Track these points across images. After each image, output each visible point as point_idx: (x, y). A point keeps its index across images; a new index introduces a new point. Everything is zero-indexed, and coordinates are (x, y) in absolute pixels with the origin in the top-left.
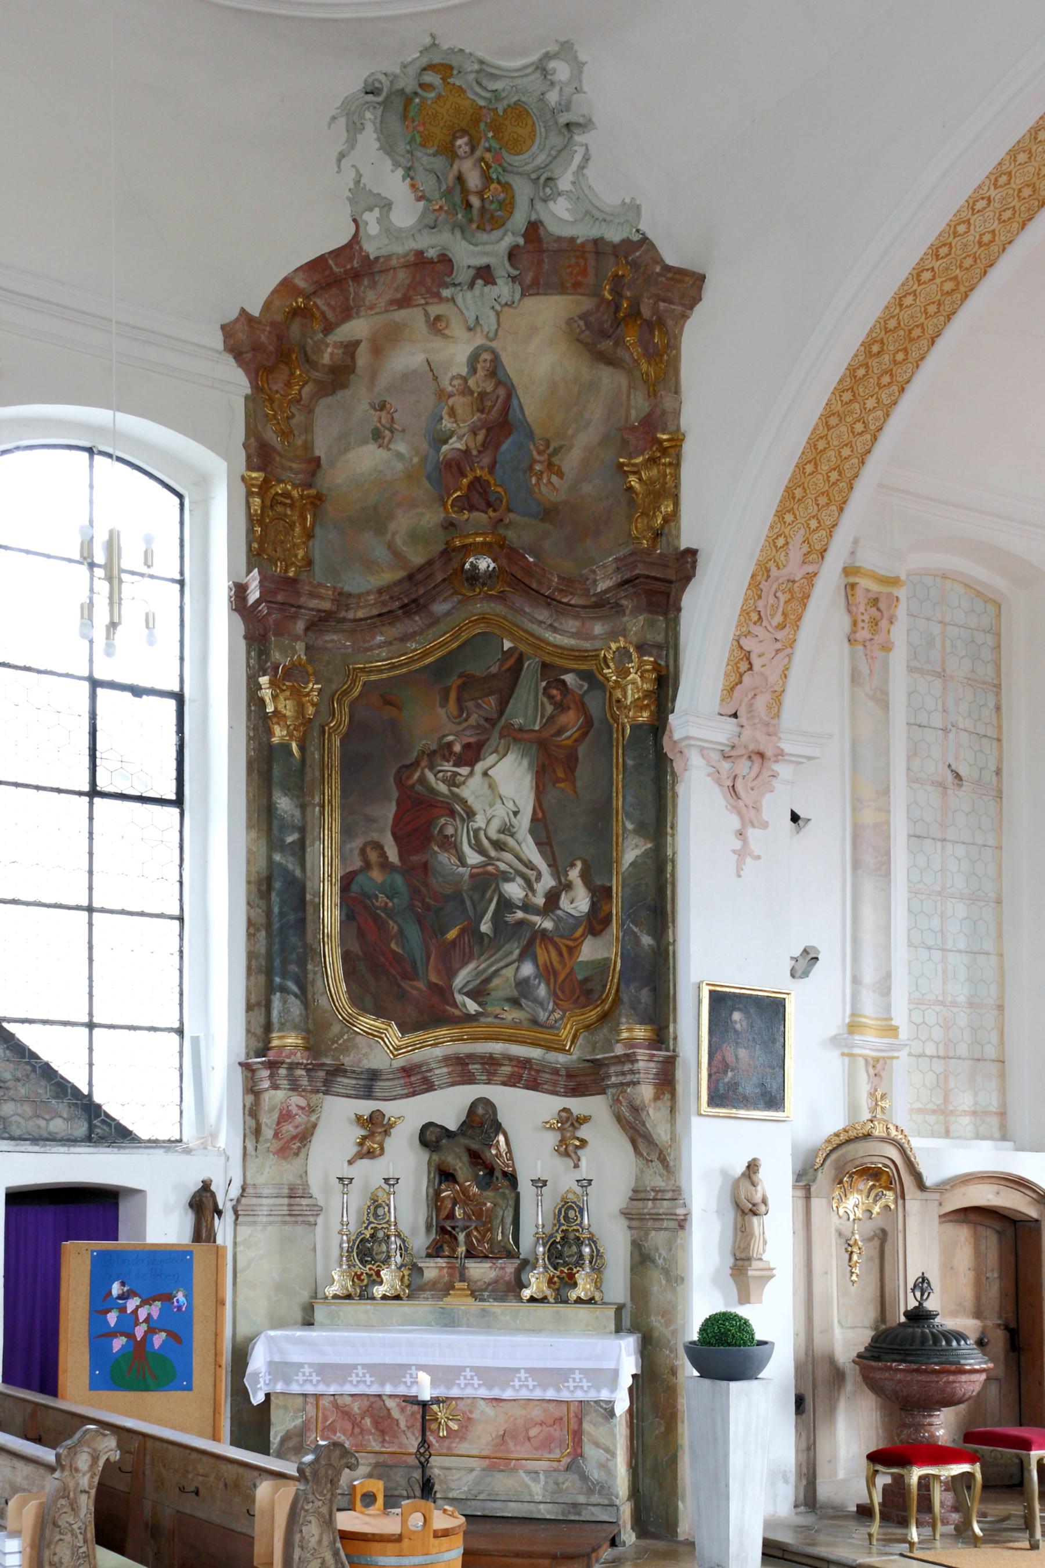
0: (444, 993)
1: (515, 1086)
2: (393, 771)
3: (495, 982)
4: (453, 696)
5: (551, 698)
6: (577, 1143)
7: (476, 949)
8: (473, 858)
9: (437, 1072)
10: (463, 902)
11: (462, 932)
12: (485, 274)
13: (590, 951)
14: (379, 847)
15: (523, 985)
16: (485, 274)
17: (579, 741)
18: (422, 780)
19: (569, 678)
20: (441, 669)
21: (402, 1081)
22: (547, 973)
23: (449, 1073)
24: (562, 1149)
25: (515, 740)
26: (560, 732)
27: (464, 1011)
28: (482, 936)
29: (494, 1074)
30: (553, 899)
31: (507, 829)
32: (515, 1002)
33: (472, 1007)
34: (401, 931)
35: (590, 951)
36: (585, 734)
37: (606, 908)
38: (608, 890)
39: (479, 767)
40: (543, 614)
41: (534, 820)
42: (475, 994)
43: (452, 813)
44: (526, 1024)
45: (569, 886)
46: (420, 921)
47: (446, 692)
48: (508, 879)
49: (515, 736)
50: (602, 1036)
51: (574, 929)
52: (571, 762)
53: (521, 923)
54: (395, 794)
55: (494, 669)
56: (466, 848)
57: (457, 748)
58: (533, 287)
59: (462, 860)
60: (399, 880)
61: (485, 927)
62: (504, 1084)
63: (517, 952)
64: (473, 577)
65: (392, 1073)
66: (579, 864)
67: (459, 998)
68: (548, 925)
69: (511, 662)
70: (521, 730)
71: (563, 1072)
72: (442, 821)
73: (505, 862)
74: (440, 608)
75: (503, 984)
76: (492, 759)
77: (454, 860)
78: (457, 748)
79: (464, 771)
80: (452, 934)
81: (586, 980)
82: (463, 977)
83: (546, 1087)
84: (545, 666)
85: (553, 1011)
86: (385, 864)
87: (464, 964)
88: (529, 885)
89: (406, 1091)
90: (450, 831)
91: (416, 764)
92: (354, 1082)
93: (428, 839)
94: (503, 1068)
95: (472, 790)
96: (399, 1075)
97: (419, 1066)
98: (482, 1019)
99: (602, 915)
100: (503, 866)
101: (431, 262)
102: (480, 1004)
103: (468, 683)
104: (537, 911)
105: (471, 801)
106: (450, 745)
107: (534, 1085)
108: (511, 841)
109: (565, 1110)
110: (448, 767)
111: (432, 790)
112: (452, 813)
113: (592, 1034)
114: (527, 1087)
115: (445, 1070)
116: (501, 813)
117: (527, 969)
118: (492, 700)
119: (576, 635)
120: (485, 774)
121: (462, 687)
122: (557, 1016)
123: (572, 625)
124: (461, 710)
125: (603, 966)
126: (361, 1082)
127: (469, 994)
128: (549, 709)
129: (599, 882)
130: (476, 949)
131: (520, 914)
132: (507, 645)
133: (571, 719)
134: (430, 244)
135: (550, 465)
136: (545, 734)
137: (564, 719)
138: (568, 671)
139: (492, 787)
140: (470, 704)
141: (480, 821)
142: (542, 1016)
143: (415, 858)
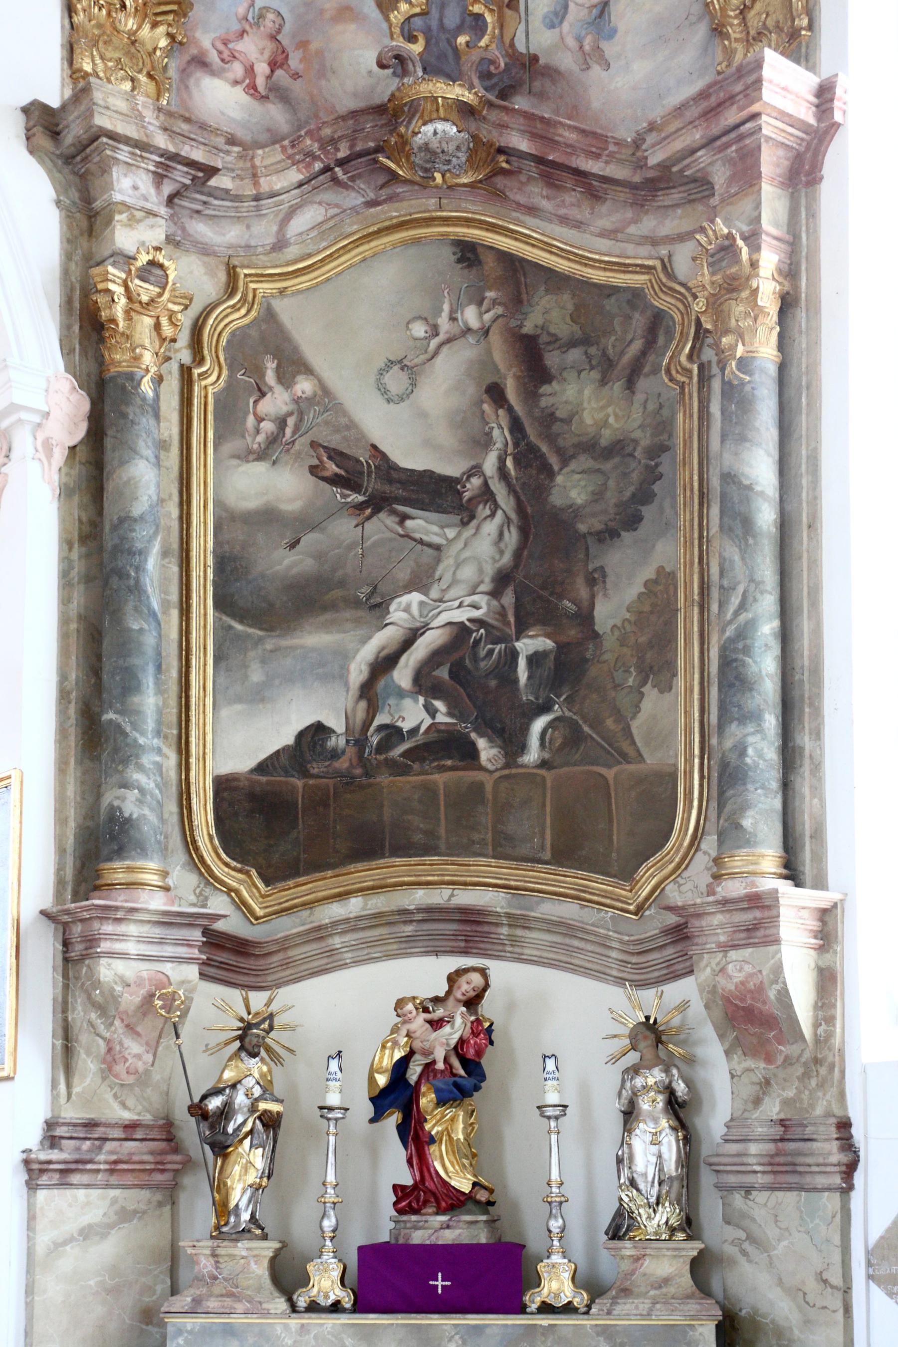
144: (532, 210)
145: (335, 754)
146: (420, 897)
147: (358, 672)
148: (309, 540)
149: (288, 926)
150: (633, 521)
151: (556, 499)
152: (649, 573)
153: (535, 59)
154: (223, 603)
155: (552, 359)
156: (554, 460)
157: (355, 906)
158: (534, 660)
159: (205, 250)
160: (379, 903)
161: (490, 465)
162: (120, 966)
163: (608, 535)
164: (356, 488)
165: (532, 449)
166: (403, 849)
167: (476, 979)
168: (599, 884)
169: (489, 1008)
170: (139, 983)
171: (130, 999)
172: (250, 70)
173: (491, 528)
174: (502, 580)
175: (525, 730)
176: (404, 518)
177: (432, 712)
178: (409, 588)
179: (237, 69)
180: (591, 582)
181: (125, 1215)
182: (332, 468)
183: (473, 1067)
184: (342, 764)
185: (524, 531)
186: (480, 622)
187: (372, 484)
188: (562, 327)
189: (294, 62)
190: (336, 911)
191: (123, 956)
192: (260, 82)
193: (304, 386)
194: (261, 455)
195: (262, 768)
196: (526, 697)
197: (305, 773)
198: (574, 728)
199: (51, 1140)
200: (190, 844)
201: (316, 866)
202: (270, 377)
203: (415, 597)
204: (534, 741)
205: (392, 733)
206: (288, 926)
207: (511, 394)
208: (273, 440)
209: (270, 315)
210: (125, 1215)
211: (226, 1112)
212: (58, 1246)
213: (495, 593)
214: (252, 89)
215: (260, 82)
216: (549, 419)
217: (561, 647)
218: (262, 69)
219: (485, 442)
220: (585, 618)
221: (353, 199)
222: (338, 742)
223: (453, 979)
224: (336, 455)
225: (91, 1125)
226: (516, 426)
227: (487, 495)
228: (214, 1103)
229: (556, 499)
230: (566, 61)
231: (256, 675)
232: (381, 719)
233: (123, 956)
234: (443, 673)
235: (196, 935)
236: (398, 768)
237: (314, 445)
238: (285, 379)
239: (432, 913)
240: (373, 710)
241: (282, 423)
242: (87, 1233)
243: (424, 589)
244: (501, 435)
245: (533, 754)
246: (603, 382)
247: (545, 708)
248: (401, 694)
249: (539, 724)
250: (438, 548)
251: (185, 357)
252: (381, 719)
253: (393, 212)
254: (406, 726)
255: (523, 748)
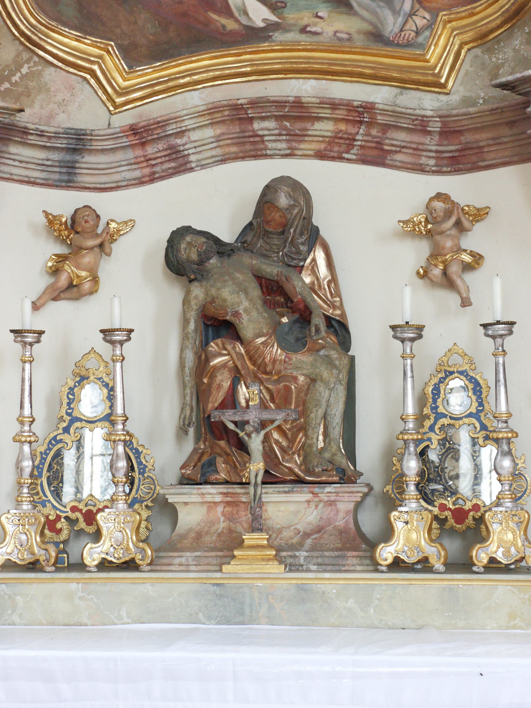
1: (340, 158)
6: (467, 258)
9: (195, 136)
21: (130, 155)
23: (218, 139)
24: (437, 272)
27: (244, 20)
44: (359, 40)
50: (510, 53)
62: (321, 156)
65: (113, 137)
71: (435, 126)
83: (399, 157)
85: (412, 14)
89: (137, 174)
92: (41, 155)
94: (318, 125)
96: (125, 141)
97: (162, 124)
98: (278, 36)
102: (273, 8)
109: (439, 196)
113: (490, 51)
114: (364, 161)
115: (209, 133)
122: (420, 22)
126: (56, 156)
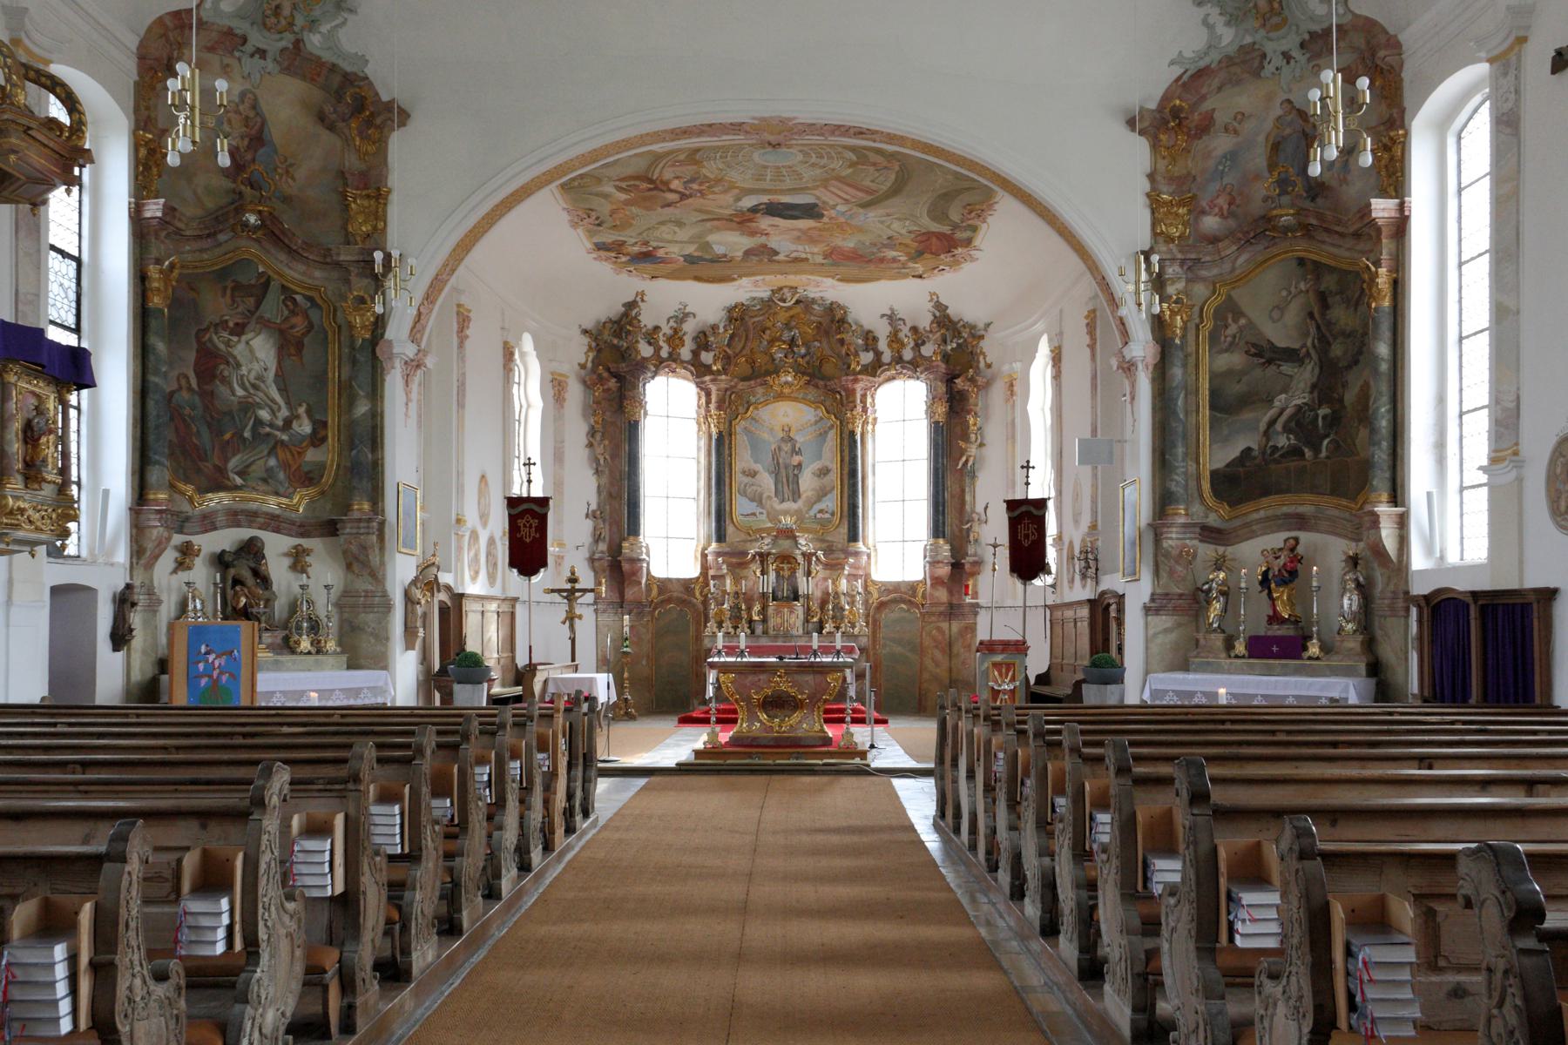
0: (221, 471)
2: (194, 332)
3: (253, 467)
4: (229, 292)
5: (287, 306)
7: (241, 447)
8: (240, 392)
10: (233, 418)
11: (234, 435)
12: (262, 53)
13: (311, 455)
14: (187, 377)
15: (269, 470)
16: (262, 53)
17: (304, 335)
18: (210, 340)
19: (298, 298)
20: (223, 274)
22: (285, 465)
25: (265, 326)
26: (292, 327)
28: (245, 440)
29: (251, 522)
30: (288, 424)
31: (260, 378)
32: (265, 481)
33: (239, 481)
34: (198, 431)
35: (311, 455)
36: (309, 332)
37: (322, 433)
38: (325, 424)
39: (244, 338)
40: (283, 256)
41: (276, 375)
42: (241, 474)
43: (228, 363)
45: (298, 417)
46: (209, 426)
47: (225, 289)
48: (261, 408)
49: (265, 324)
51: (301, 442)
52: (300, 346)
53: (268, 435)
54: (195, 345)
55: (253, 282)
56: (236, 386)
57: (231, 324)
58: (288, 70)
59: (233, 393)
60: (197, 399)
61: (247, 434)
63: (266, 452)
64: (246, 225)
66: (305, 406)
67: (232, 475)
68: (285, 437)
69: (262, 280)
70: (269, 321)
72: (222, 367)
73: (259, 397)
74: (222, 237)
75: (257, 470)
76: (250, 336)
77: (228, 391)
78: (231, 324)
79: (235, 339)
80: (227, 436)
81: (309, 472)
82: (234, 463)
84: (283, 286)
86: (190, 389)
87: (234, 455)
88: (273, 413)
90: (226, 373)
91: (207, 330)
93: (214, 377)
95: (239, 350)
99: (319, 436)
100: (258, 400)
101: (236, 35)
103: (238, 287)
104: (278, 429)
105: (239, 357)
106: (226, 321)
107: (277, 530)
108: (262, 385)
110: (225, 334)
111: (216, 347)
112: (228, 363)
116: (256, 367)
117: (272, 462)
118: (252, 300)
119: (304, 274)
120: (247, 343)
121: (233, 289)
123: (301, 268)
124: (233, 301)
125: (322, 467)
127: (237, 474)
128: (286, 313)
129: (318, 417)
130: (241, 447)
131: (268, 429)
132: (261, 269)
133: (299, 323)
134: (241, 27)
135: (287, 172)
136: (284, 326)
137: (294, 320)
138: (297, 293)
139: (252, 351)
140: (238, 299)
141: (244, 371)
142: (282, 490)
143: (206, 387)
144: (1323, 242)
145: (1255, 458)
146: (1285, 509)
147: (1262, 426)
148: (1245, 379)
149: (1237, 523)
150: (1356, 362)
151: (1332, 355)
152: (1360, 383)
153: (1323, 183)
154: (1213, 407)
155: (1330, 300)
156: (1331, 339)
157: (1262, 514)
158: (1324, 418)
159: (1204, 279)
160: (1270, 512)
161: (1309, 343)
162: (1170, 542)
163: (1349, 367)
164: (1262, 357)
165: (1323, 336)
166: (1280, 492)
167: (1292, 542)
168: (1344, 502)
169: (1300, 550)
170: (1177, 546)
171: (1175, 552)
172: (1221, 209)
173: (1309, 367)
174: (1314, 387)
175: (1321, 443)
176: (1279, 366)
177: (1289, 439)
178: (1281, 393)
179: (1216, 210)
180: (1343, 386)
181: (1180, 625)
182: (1253, 350)
183: (1293, 574)
184: (1257, 461)
185: (1321, 368)
186: (1305, 404)
187: (1268, 355)
188: (1333, 288)
189: (1238, 202)
190: (1255, 516)
191: (1171, 538)
192: (1225, 212)
193: (1243, 321)
194: (1226, 351)
195: (1228, 465)
196: (1322, 431)
197: (1243, 466)
198: (1337, 442)
199: (1152, 600)
200: (1201, 496)
201: (1248, 499)
202: (1230, 321)
203: (1284, 396)
204: (1324, 449)
205: (1275, 448)
206: (1237, 523)
207: (1317, 315)
208: (1231, 344)
209: (1229, 297)
210: (1180, 625)
211: (1210, 590)
212: (1155, 635)
213: (1311, 392)
214: (1222, 216)
215: (1225, 212)
216: (1329, 324)
217: (1333, 412)
218: (1225, 207)
219: (1307, 334)
220: (1341, 400)
221: (1260, 247)
222: (1256, 453)
223: (1286, 541)
224: (1254, 345)
225: (1167, 594)
226: (1318, 327)
227: (1308, 354)
228: (1206, 587)
229: (1332, 355)
230: (1334, 183)
231: (1226, 432)
232: (1271, 444)
233: (1171, 538)
234: (1293, 424)
235: (1198, 530)
236: (1277, 462)
237: (1247, 343)
238: (1235, 321)
239: (1287, 516)
240: (1268, 440)
241: (1234, 337)
242: (1166, 631)
243: (1286, 392)
244: (1313, 331)
245: (1324, 454)
246: (1347, 308)
247: (1327, 436)
248: (1278, 433)
249: (1325, 442)
250: (1291, 376)
251: (1197, 321)
252: (1271, 444)
253: (1275, 250)
254: (1280, 445)
255: (1320, 451)
